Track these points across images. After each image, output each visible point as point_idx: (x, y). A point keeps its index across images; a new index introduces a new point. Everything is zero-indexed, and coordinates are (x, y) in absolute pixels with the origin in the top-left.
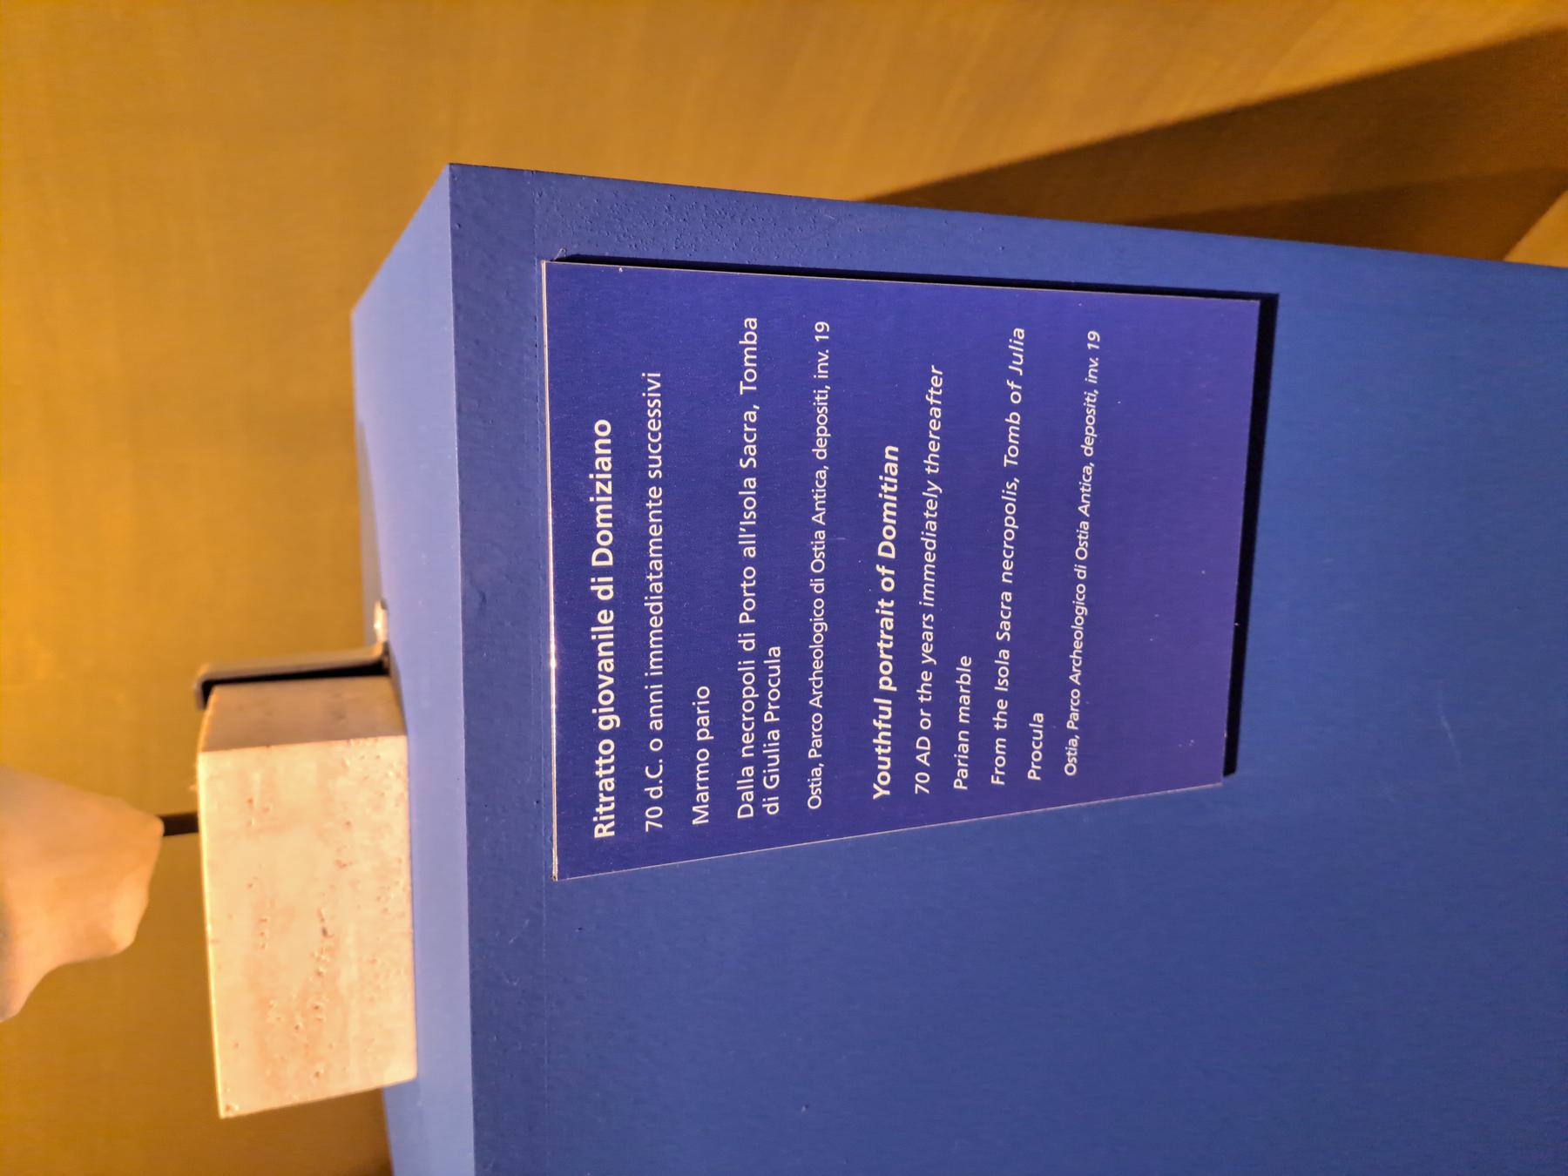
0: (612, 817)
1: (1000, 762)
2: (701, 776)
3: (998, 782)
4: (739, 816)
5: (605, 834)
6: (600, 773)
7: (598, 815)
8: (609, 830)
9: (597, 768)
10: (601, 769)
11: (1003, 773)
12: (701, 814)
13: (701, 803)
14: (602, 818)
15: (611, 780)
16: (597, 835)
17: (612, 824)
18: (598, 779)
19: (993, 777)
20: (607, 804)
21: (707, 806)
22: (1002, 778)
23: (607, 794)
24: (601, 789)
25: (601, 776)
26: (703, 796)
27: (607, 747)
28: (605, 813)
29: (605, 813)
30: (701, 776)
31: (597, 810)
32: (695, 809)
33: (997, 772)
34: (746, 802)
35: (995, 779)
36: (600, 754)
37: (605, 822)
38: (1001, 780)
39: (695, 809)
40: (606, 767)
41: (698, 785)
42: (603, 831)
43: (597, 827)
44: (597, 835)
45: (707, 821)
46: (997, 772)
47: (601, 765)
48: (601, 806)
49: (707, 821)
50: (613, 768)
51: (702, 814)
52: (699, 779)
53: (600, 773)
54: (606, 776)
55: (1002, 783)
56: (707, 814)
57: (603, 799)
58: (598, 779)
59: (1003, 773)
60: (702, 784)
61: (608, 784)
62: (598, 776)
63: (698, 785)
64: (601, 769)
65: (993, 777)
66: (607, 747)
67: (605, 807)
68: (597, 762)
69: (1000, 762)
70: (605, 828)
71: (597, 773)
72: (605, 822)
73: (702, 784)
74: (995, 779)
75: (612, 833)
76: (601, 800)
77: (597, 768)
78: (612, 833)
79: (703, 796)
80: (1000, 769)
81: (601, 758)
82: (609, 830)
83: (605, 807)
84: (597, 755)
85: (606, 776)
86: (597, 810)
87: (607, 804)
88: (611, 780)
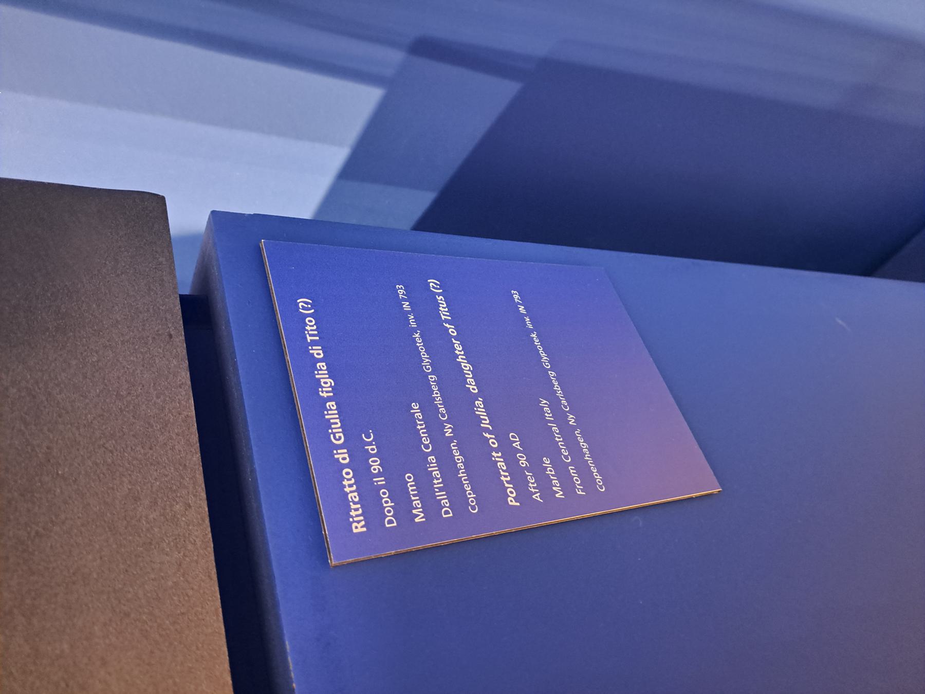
0: (362, 518)
2: (412, 490)
3: (581, 493)
4: (444, 516)
5: (360, 530)
6: (347, 490)
7: (352, 517)
8: (362, 527)
10: (347, 487)
11: (582, 487)
12: (419, 515)
13: (417, 508)
14: (356, 519)
15: (356, 494)
16: (355, 531)
17: (363, 523)
19: (577, 490)
20: (356, 510)
21: (421, 510)
23: (355, 503)
24: (350, 500)
25: (348, 492)
26: (417, 503)
27: (348, 473)
28: (357, 516)
29: (357, 516)
30: (412, 490)
31: (351, 513)
32: (414, 511)
34: (445, 507)
35: (579, 491)
36: (345, 478)
37: (358, 522)
38: (582, 492)
39: (414, 511)
40: (350, 486)
41: (411, 496)
42: (358, 528)
43: (354, 525)
44: (355, 531)
45: (424, 520)
46: (578, 487)
47: (347, 485)
48: (353, 511)
49: (424, 520)
50: (354, 486)
51: (419, 515)
52: (411, 493)
54: (351, 492)
56: (422, 515)
57: (353, 506)
59: (582, 487)
60: (414, 495)
61: (354, 496)
62: (346, 492)
63: (411, 496)
64: (347, 487)
65: (577, 490)
66: (348, 473)
67: (356, 511)
68: (344, 483)
70: (359, 525)
71: (345, 489)
72: (358, 522)
73: (414, 495)
74: (579, 491)
75: (364, 529)
76: (352, 507)
78: (364, 529)
79: (417, 503)
80: (578, 485)
81: (345, 480)
82: (362, 527)
83: (356, 511)
84: (343, 478)
85: (351, 492)
86: (351, 513)
87: (356, 510)
88: (356, 494)
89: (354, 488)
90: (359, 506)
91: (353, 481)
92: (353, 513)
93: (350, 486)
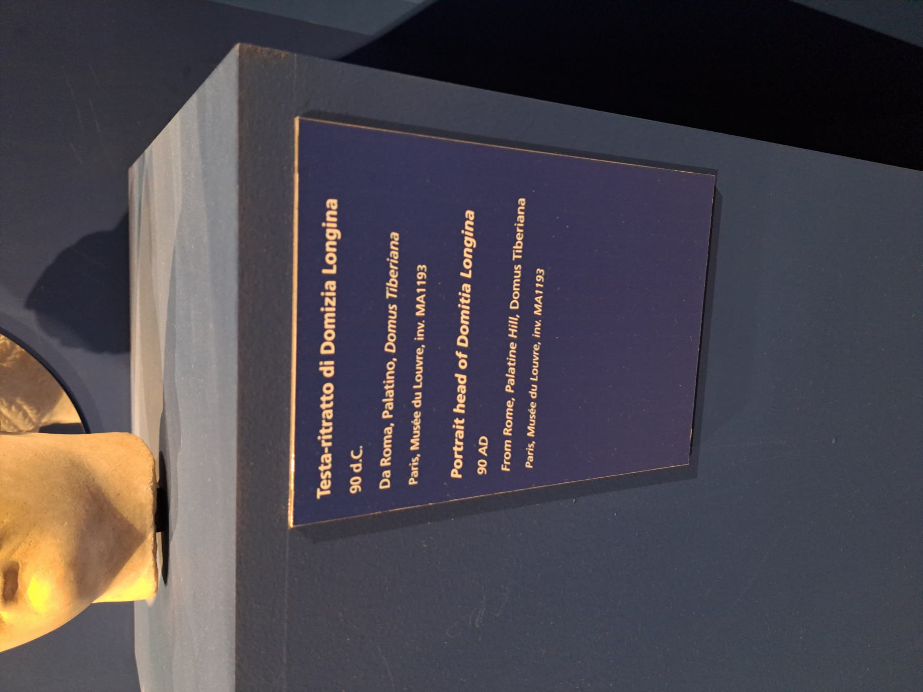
1: (508, 456)
9: (321, 402)
11: (509, 463)
18: (322, 411)
20: (327, 428)
22: (508, 466)
23: (327, 421)
29: (326, 434)
33: (505, 462)
38: (508, 468)
40: (328, 402)
53: (323, 406)
55: (508, 470)
58: (322, 411)
59: (509, 463)
61: (328, 414)
69: (508, 456)
77: (321, 402)
80: (507, 461)
87: (327, 428)
89: (331, 404)
90: (330, 424)
91: (332, 397)
92: (323, 431)
93: (328, 402)
